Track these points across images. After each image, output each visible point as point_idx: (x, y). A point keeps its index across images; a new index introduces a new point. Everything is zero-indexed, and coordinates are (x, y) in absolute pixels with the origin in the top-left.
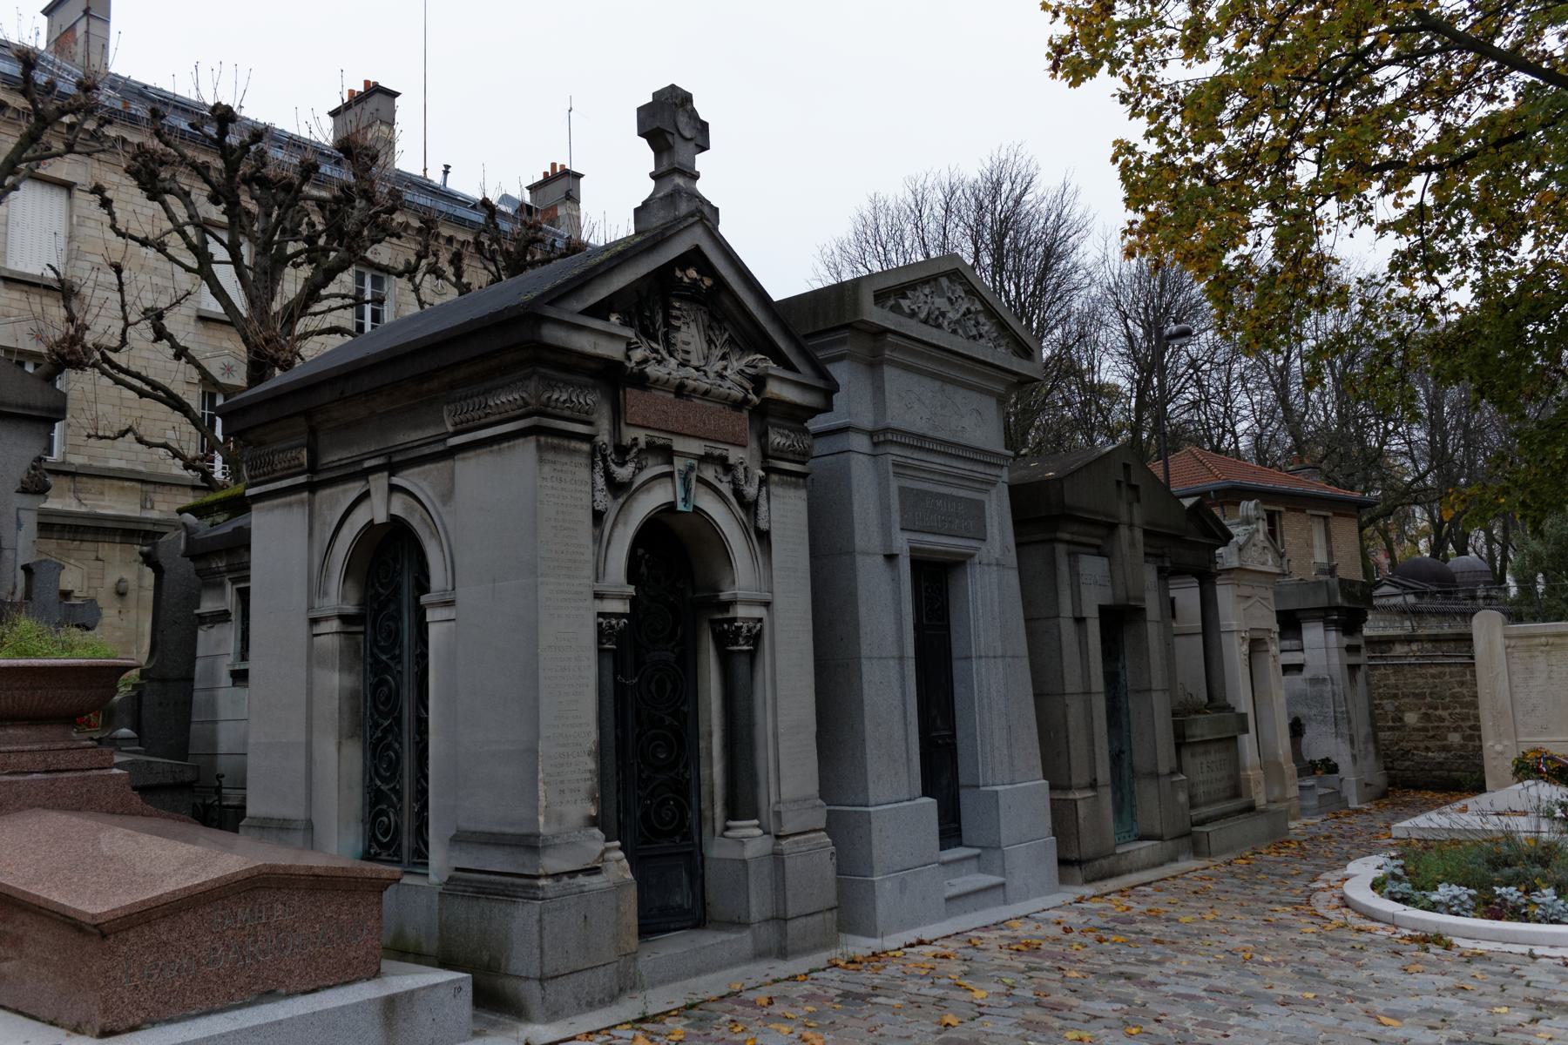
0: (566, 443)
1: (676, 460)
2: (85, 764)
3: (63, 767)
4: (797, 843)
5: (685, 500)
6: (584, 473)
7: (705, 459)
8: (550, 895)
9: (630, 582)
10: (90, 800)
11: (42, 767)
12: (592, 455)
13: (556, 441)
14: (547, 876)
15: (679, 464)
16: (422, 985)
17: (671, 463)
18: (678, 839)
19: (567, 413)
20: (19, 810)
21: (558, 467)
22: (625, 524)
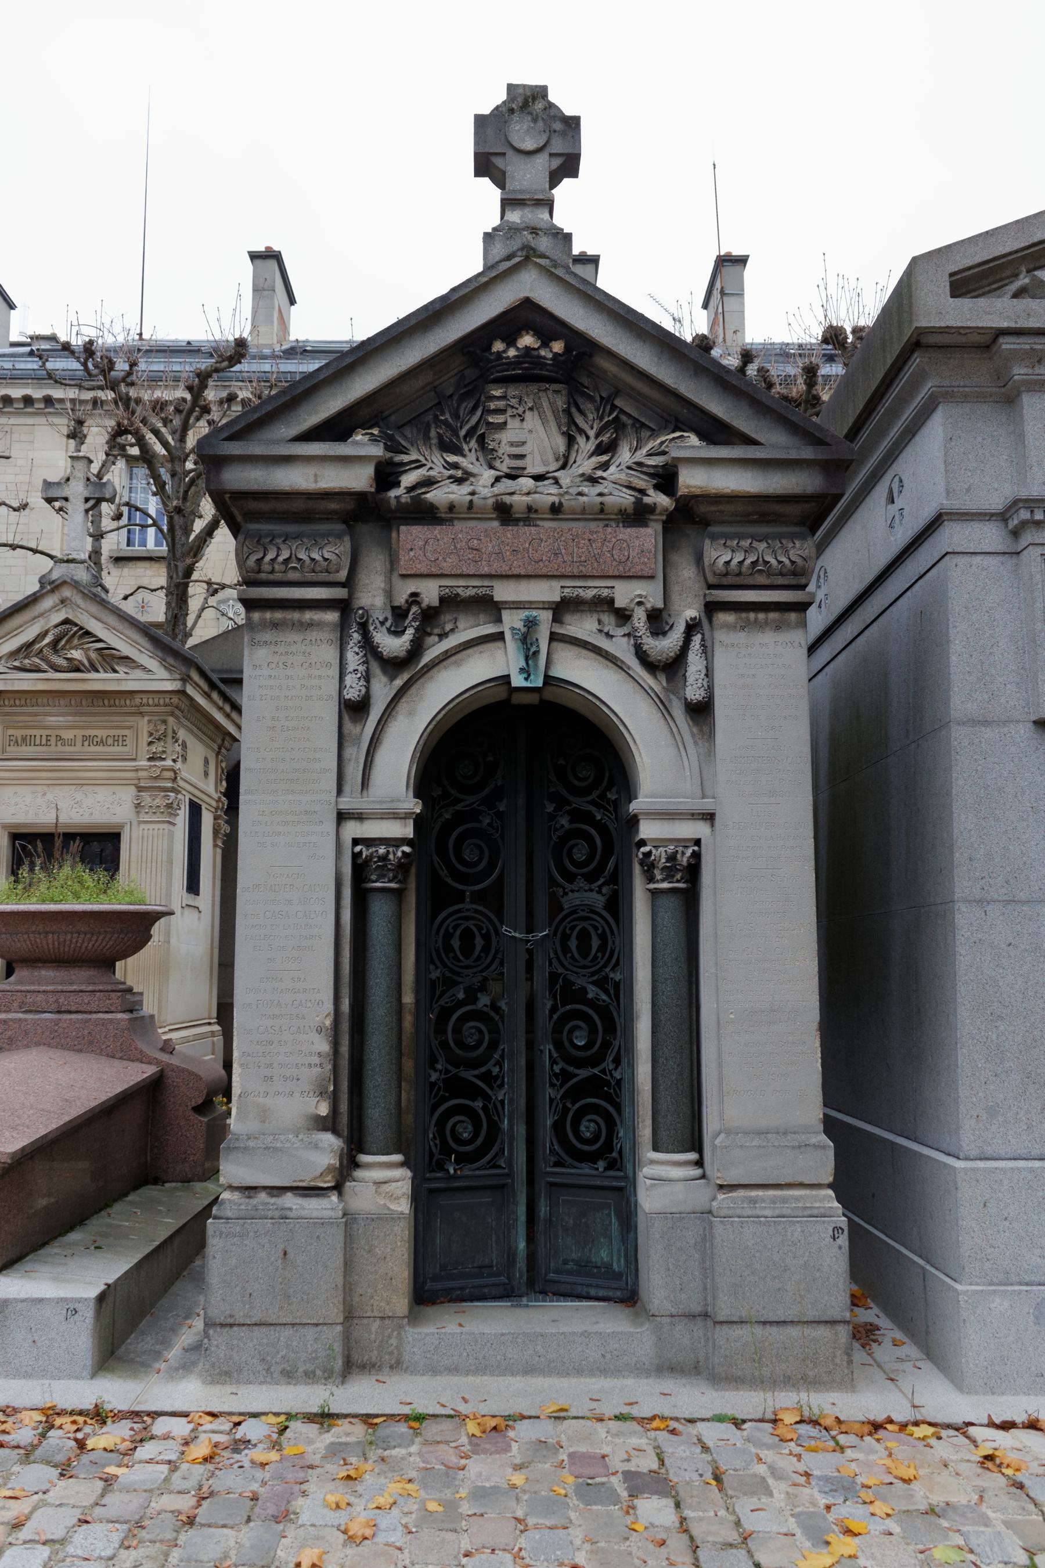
0: (296, 615)
1: (506, 615)
2: (93, 1006)
3: (73, 1008)
4: (754, 1201)
5: (526, 672)
6: (329, 653)
7: (561, 609)
8: (229, 1214)
9: (418, 795)
10: (91, 1043)
11: (54, 1007)
12: (343, 627)
13: (278, 615)
14: (231, 1188)
15: (512, 621)
16: (23, 1295)
17: (499, 620)
18: (601, 1165)
19: (293, 576)
20: (27, 1046)
21: (281, 649)
22: (411, 713)
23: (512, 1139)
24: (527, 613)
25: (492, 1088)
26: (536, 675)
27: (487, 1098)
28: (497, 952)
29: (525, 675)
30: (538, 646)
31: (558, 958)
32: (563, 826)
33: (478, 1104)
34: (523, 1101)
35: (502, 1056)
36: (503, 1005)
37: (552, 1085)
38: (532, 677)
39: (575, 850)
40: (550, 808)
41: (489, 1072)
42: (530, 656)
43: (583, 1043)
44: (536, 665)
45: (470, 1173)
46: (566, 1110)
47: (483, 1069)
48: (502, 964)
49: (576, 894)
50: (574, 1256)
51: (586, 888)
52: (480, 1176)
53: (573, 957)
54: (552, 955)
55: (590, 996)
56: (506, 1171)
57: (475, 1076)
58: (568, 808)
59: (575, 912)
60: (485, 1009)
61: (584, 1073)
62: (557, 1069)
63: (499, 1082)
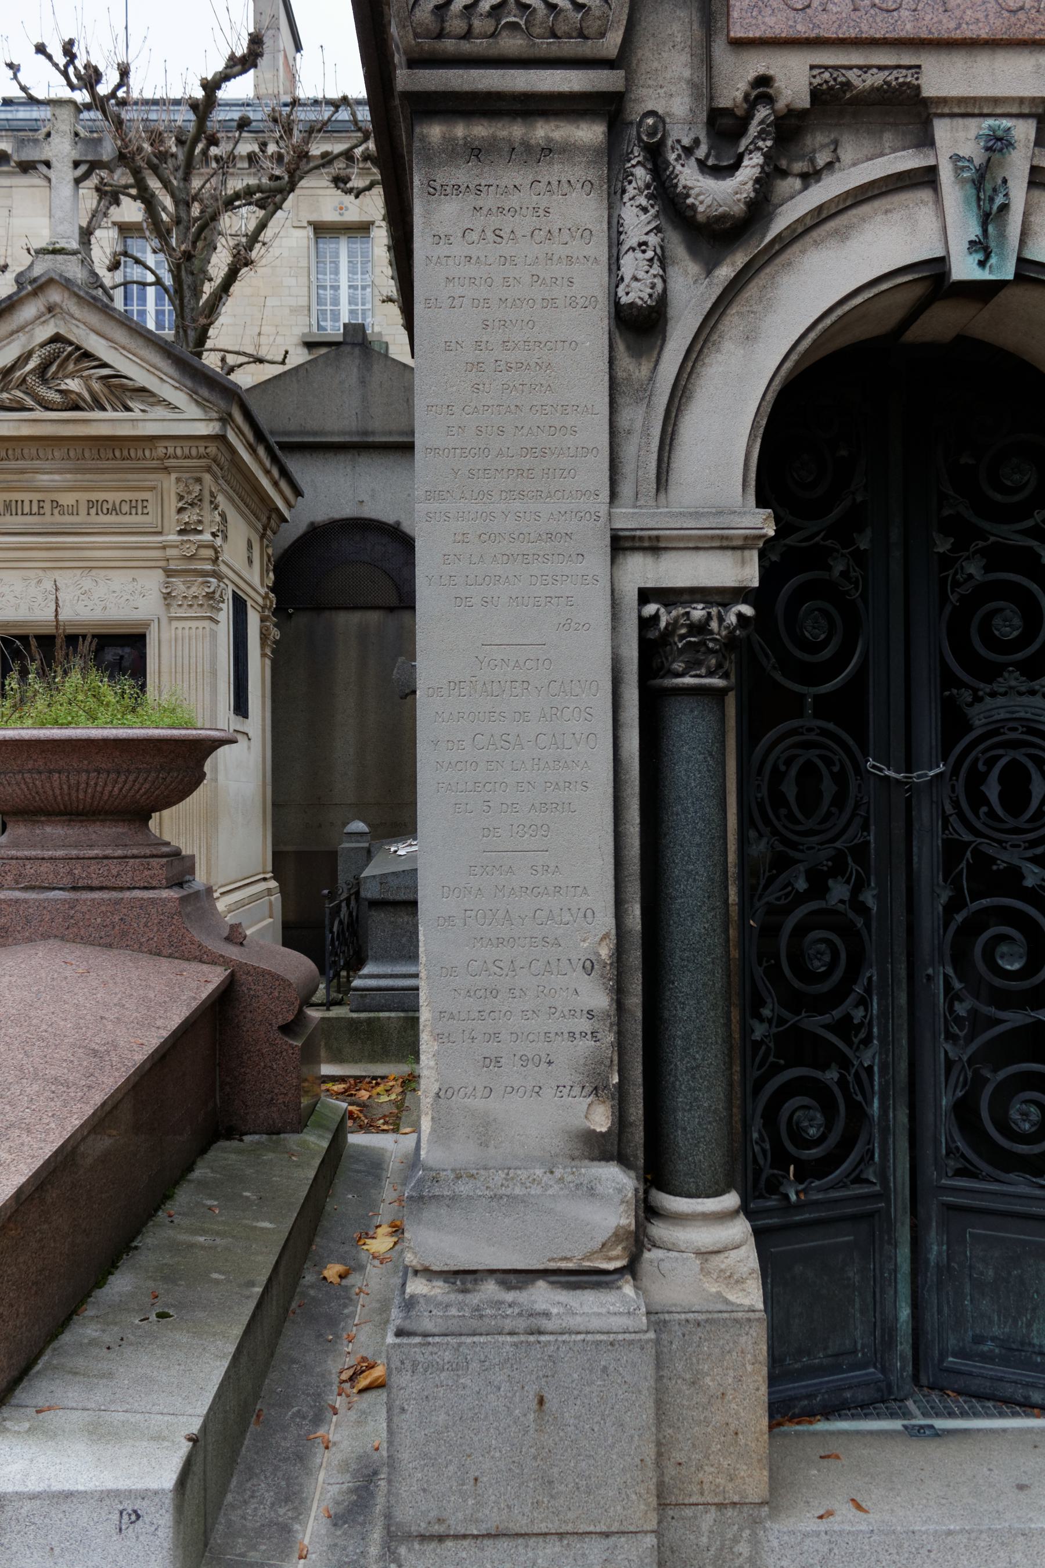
0: (516, 131)
1: (943, 130)
2: (126, 880)
3: (96, 883)
5: (982, 248)
6: (585, 209)
8: (428, 1325)
9: (761, 502)
10: (124, 934)
11: (67, 881)
12: (613, 154)
13: (481, 130)
14: (427, 1273)
15: (956, 141)
17: (927, 141)
19: (511, 44)
20: (30, 940)
21: (489, 201)
22: (750, 337)
23: (885, 1131)
24: (991, 122)
25: (850, 1044)
26: (1002, 257)
27: (845, 1064)
28: (857, 806)
29: (980, 256)
30: (1006, 195)
31: (961, 815)
32: (970, 576)
33: (831, 1076)
34: (903, 1066)
35: (868, 990)
36: (869, 898)
37: (950, 1037)
38: (993, 260)
39: (997, 621)
40: (943, 545)
41: (848, 1018)
42: (991, 216)
43: (1016, 966)
44: (1002, 235)
45: (820, 1196)
46: (978, 1082)
47: (837, 1013)
48: (865, 827)
49: (1001, 701)
50: (996, 1331)
51: (1023, 689)
52: (836, 1201)
53: (992, 814)
54: (949, 809)
55: (1029, 882)
56: (878, 1188)
57: (825, 1027)
58: (981, 544)
59: (996, 732)
60: (841, 907)
61: (1014, 1018)
62: (961, 1009)
63: (862, 1035)
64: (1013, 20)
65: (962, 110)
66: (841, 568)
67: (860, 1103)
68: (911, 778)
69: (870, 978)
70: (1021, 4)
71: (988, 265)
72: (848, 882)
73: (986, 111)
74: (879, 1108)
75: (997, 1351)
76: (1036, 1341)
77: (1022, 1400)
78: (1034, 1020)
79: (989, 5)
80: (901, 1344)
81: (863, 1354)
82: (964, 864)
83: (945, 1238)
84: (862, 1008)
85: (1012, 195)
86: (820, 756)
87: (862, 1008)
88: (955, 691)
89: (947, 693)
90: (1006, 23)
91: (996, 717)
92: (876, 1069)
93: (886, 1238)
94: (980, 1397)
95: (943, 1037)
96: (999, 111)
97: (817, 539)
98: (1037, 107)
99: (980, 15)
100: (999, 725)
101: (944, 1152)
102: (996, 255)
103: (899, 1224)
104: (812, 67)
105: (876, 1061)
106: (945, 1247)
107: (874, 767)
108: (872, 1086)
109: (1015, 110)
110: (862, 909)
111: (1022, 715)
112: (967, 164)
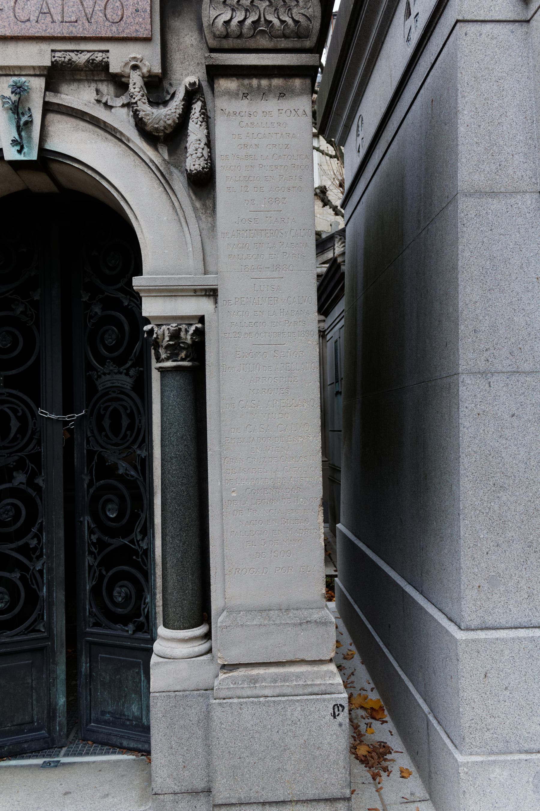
4: (254, 680)
7: (56, 75)
18: (131, 627)
23: (51, 604)
24: (15, 79)
25: (31, 560)
26: (30, 148)
27: (24, 568)
28: (33, 433)
29: (18, 148)
30: (31, 116)
31: (94, 436)
32: (96, 313)
33: (15, 576)
34: (61, 570)
35: (40, 530)
36: (40, 481)
37: (91, 553)
38: (25, 150)
39: (106, 336)
40: (85, 298)
41: (27, 544)
42: (24, 127)
43: (115, 515)
44: (30, 137)
45: (7, 640)
46: (102, 577)
47: (21, 543)
48: (39, 443)
49: (108, 377)
50: (110, 709)
51: (116, 371)
52: (17, 642)
53: (106, 436)
54: (89, 434)
55: (121, 471)
56: (46, 634)
57: (12, 549)
58: (101, 296)
59: (107, 394)
60: (22, 486)
61: (117, 542)
62: (94, 538)
63: (38, 553)
64: (23, 26)
65: (4, 73)
66: (21, 309)
67: (35, 589)
68: (65, 418)
69: (42, 522)
70: (28, 18)
71: (23, 152)
72: (26, 473)
73: (16, 73)
74: (46, 592)
75: (111, 719)
76: (126, 713)
77: (119, 745)
78: (123, 543)
79: (10, 19)
80: (60, 717)
81: (38, 724)
82: (94, 463)
83: (88, 660)
84: (36, 539)
85: (34, 116)
86: (8, 408)
87: (36, 539)
88: (90, 373)
89: (88, 374)
90: (20, 28)
91: (107, 386)
92: (45, 571)
93: (51, 661)
94: (103, 744)
95: (87, 553)
96: (23, 73)
97: (7, 295)
98: (43, 71)
99: (6, 24)
100: (108, 390)
101: (88, 614)
102: (27, 147)
103: (58, 653)
104: (53, 51)
105: (45, 567)
106: (88, 665)
107: (42, 412)
108: (43, 581)
109: (32, 72)
110: (38, 489)
111: (117, 384)
112: (8, 100)
